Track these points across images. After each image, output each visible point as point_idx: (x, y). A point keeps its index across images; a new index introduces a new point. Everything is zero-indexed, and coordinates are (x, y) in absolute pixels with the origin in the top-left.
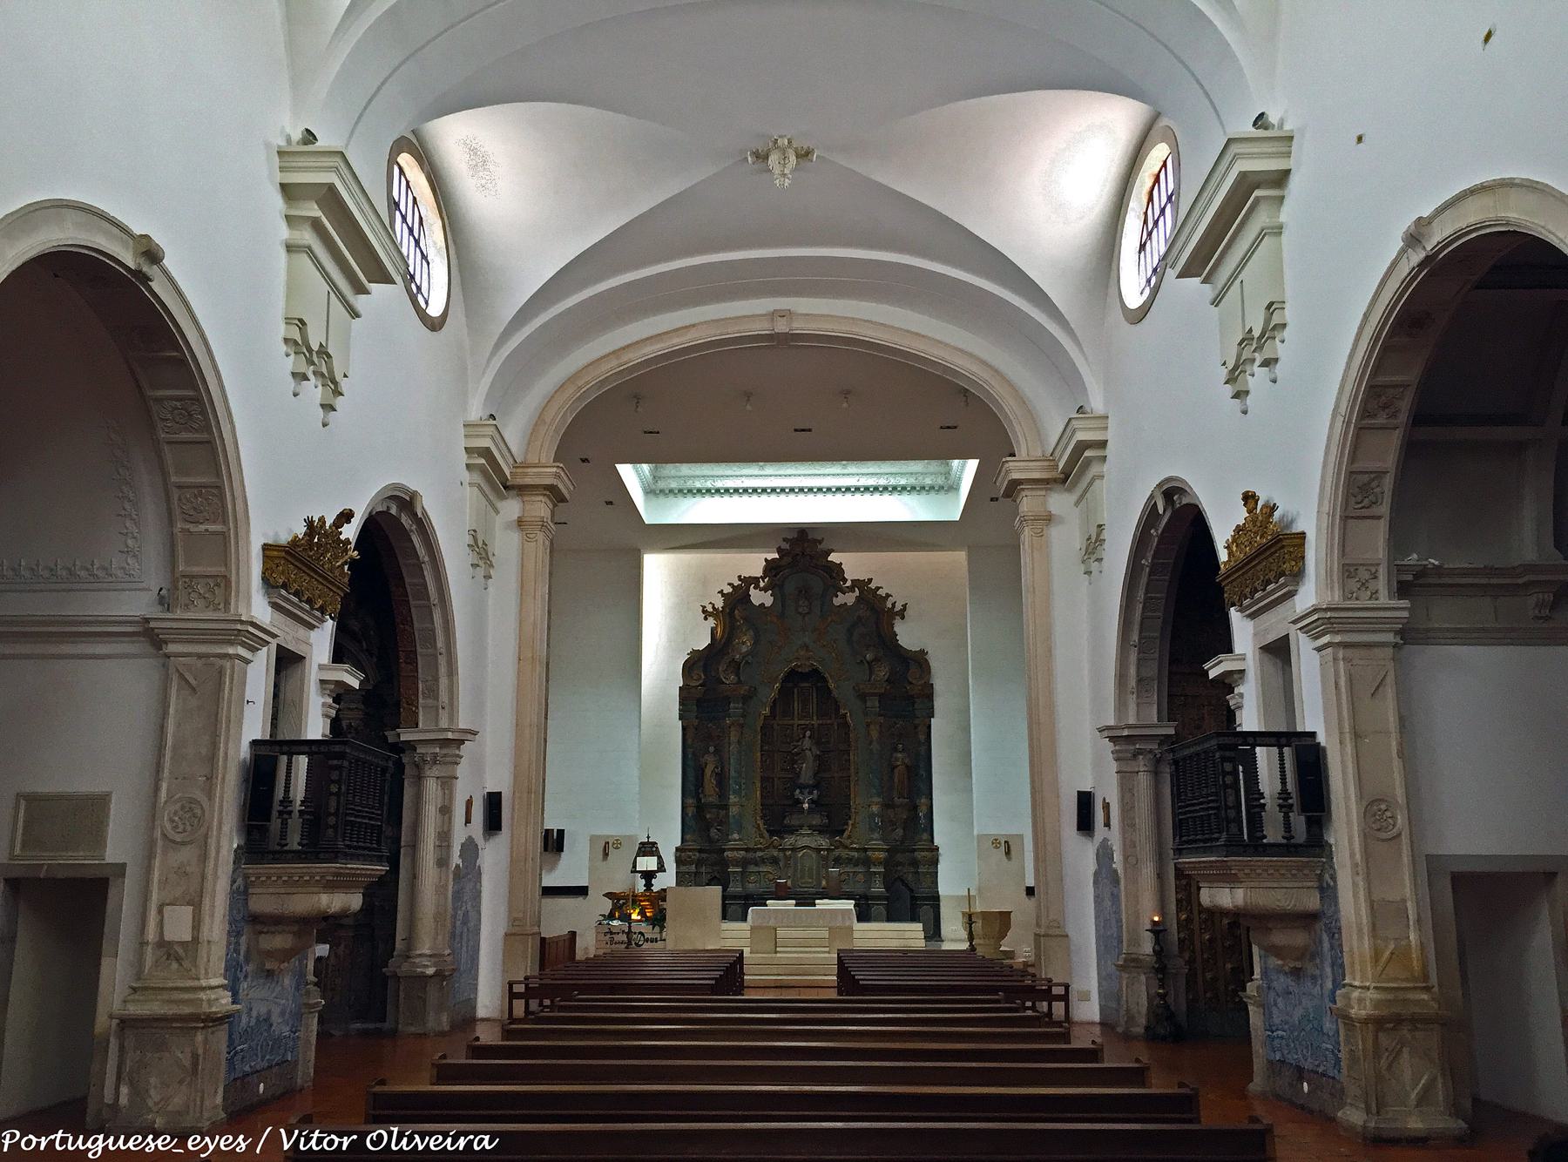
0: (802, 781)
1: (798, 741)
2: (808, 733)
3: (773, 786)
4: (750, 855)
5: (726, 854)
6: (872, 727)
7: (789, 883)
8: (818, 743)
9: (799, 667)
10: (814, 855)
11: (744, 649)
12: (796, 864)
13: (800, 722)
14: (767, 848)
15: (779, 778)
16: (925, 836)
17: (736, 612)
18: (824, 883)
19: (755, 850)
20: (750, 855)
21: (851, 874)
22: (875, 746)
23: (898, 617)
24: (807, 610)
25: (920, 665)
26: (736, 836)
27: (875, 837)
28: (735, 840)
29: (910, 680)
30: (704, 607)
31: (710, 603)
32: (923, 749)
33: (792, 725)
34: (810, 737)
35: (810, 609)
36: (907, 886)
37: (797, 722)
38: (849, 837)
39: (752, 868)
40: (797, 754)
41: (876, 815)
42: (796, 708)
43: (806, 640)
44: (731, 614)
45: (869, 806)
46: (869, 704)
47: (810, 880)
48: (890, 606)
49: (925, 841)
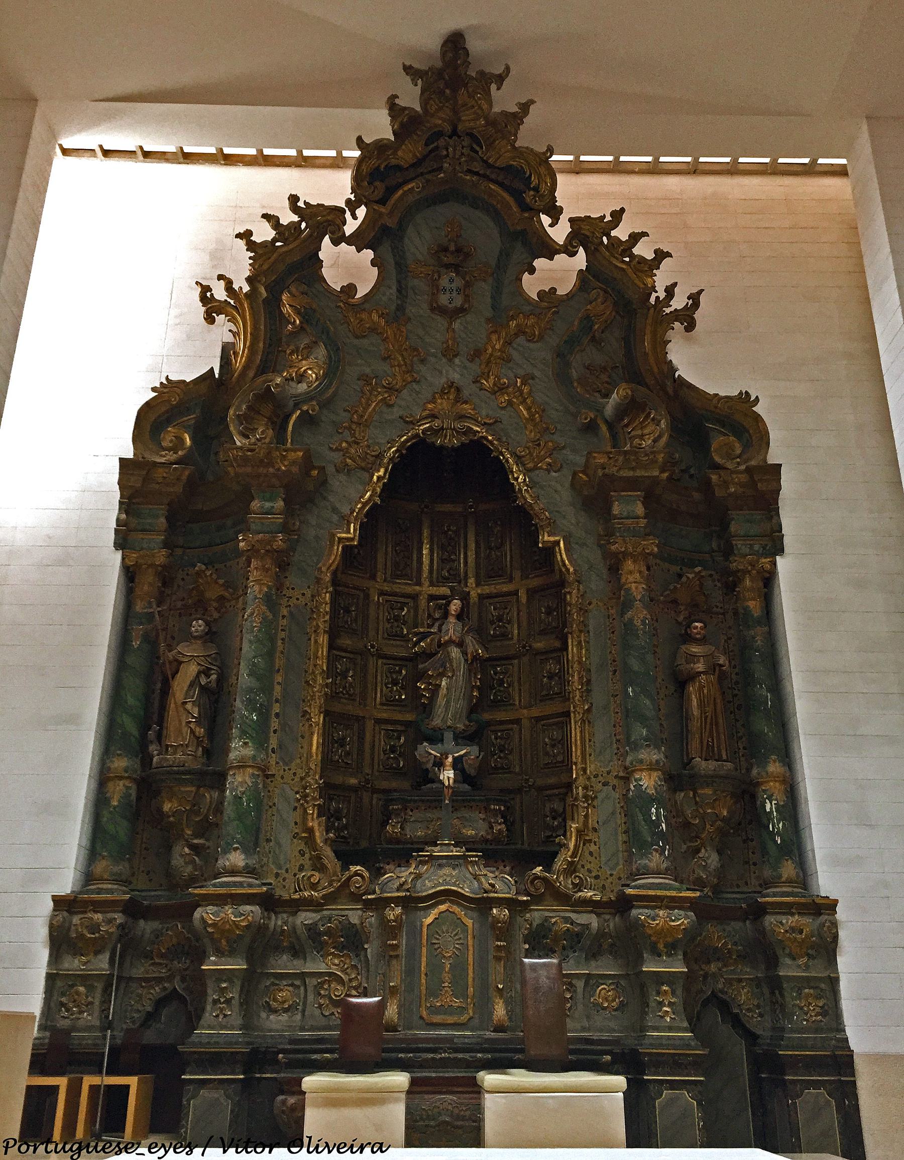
0: (437, 722)
1: (430, 626)
2: (455, 606)
3: (361, 738)
4: (277, 922)
5: (197, 914)
6: (629, 565)
7: (392, 1011)
8: (480, 632)
9: (437, 432)
10: (469, 922)
11: (303, 387)
12: (413, 953)
13: (434, 591)
14: (331, 898)
15: (378, 721)
16: (788, 869)
17: (285, 297)
18: (500, 1011)
19: (296, 906)
20: (277, 922)
21: (580, 984)
22: (639, 615)
23: (677, 325)
24: (458, 301)
25: (738, 430)
26: (237, 859)
27: (653, 865)
28: (233, 872)
29: (717, 459)
30: (205, 290)
31: (220, 277)
32: (758, 635)
33: (415, 597)
34: (459, 617)
35: (467, 296)
36: (737, 1022)
37: (427, 589)
38: (571, 869)
39: (284, 964)
40: (427, 655)
41: (652, 800)
42: (426, 560)
43: (456, 376)
44: (273, 303)
45: (626, 779)
46: (616, 509)
47: (457, 1002)
48: (662, 295)
49: (790, 881)
